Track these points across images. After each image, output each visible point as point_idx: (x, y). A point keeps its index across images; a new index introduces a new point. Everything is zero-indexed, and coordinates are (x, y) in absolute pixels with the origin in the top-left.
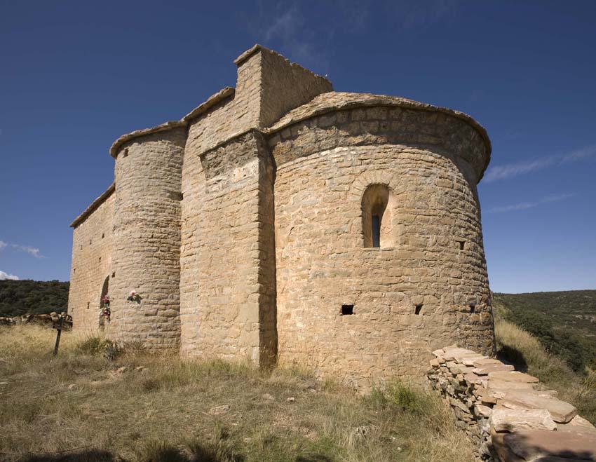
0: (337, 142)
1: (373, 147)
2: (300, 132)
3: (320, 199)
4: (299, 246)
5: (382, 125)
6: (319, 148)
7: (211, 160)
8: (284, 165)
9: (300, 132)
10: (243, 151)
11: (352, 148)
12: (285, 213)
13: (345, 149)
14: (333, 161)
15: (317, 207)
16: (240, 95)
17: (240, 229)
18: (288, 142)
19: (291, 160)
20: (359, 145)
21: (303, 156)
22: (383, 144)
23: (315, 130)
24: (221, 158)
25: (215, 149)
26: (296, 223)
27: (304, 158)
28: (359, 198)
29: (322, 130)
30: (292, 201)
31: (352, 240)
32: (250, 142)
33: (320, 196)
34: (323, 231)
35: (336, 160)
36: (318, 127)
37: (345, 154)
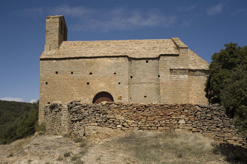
4: (195, 95)
12: (191, 87)
13: (204, 77)
16: (181, 56)
17: (183, 90)
18: (193, 72)
19: (192, 76)
25: (177, 69)
30: (193, 85)
32: (187, 71)
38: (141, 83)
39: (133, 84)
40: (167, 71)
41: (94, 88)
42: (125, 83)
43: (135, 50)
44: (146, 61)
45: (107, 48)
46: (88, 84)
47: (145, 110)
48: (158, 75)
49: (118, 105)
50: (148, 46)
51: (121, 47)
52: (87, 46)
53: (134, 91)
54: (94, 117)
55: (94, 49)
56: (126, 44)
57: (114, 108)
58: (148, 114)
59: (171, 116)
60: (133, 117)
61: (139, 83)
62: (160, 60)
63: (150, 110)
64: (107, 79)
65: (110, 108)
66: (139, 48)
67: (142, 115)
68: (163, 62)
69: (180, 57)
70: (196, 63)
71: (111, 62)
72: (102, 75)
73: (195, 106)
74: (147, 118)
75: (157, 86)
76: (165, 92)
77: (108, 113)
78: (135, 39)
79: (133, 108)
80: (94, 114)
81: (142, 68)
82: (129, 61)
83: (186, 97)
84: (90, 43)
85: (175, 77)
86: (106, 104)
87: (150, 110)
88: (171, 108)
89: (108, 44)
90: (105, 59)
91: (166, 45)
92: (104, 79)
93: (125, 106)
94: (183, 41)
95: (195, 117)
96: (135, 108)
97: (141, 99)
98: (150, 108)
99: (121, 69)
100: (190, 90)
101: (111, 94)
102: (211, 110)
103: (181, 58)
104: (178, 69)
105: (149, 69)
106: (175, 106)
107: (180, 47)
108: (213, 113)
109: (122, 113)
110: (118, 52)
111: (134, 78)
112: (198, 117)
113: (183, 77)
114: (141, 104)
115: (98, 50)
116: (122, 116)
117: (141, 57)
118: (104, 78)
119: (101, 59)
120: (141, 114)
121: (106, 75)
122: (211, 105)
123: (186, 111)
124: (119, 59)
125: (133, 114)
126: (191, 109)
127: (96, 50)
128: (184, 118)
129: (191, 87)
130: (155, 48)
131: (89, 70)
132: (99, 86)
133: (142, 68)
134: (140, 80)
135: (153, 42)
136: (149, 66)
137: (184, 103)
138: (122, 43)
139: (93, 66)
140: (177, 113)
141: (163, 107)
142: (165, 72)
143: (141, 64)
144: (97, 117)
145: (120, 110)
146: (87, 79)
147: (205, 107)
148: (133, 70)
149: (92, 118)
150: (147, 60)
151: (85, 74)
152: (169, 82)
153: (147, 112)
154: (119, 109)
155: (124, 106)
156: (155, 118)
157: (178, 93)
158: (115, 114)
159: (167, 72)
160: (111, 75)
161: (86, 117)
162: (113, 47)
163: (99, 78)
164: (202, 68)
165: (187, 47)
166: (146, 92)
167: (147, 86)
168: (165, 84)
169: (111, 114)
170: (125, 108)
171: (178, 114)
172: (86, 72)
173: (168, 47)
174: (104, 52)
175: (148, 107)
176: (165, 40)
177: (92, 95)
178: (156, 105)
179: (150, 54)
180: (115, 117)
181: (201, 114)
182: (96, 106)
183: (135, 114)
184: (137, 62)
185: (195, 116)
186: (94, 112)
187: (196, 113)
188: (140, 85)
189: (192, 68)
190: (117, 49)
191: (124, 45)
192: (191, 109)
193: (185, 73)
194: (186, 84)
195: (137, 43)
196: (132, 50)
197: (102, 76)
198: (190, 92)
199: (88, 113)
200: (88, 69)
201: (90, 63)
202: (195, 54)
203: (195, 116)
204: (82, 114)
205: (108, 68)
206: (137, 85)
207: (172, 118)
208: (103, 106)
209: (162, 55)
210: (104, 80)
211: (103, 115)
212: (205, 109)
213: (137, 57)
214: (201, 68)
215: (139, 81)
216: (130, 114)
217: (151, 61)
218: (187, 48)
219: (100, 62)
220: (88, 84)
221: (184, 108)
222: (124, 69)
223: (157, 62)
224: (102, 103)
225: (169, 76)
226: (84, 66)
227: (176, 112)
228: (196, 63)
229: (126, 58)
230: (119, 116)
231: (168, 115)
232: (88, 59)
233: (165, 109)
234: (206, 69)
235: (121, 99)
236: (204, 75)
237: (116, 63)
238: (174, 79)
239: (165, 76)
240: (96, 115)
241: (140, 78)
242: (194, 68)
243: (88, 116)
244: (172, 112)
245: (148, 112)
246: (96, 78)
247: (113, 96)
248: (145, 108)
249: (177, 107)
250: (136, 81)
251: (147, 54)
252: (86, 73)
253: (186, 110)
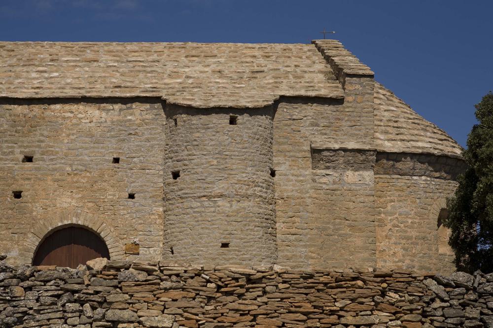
0: (425, 173)
1: (443, 181)
2: (403, 159)
4: (395, 244)
5: (452, 168)
6: (413, 173)
8: (381, 176)
9: (403, 159)
10: (361, 161)
11: (433, 179)
12: (383, 215)
13: (429, 179)
14: (421, 186)
15: (410, 218)
17: (356, 223)
18: (391, 162)
19: (388, 174)
21: (400, 175)
22: (448, 180)
23: (415, 162)
24: (337, 158)
26: (395, 226)
27: (399, 177)
29: (419, 164)
30: (389, 208)
31: (433, 246)
33: (413, 210)
34: (414, 236)
35: (422, 186)
36: (418, 161)
37: (429, 182)
38: (209, 197)
39: (181, 201)
40: (300, 155)
41: (37, 210)
42: (153, 197)
43: (188, 77)
44: (228, 117)
45: (87, 69)
46: (18, 195)
47: (246, 292)
48: (271, 169)
49: (149, 272)
50: (234, 66)
51: (137, 68)
52: (15, 60)
53: (184, 225)
54: (59, 315)
55: (42, 72)
56: (155, 57)
57: (136, 285)
58: (259, 306)
59: (341, 313)
60: (202, 316)
61: (204, 196)
62: (276, 115)
63: (265, 293)
64: (86, 179)
65: (120, 283)
66: (201, 72)
67: (237, 311)
68: (286, 125)
69: (348, 107)
70: (402, 130)
71: (103, 120)
72: (71, 165)
73: (424, 281)
74: (254, 320)
75: (265, 209)
76: (293, 230)
77: (111, 303)
78: (185, 38)
79: (203, 286)
80: (59, 304)
81: (213, 143)
82: (167, 118)
83: (367, 249)
84: (27, 49)
85: (328, 178)
86: (105, 267)
87: (265, 293)
88: (341, 287)
89: (89, 55)
90: (81, 107)
91: (296, 66)
92: (75, 180)
93: (174, 278)
94: (354, 53)
95: (423, 320)
96: (213, 285)
97: (211, 254)
98: (264, 285)
99: (138, 146)
100: (378, 226)
101: (102, 235)
102: (481, 295)
103: (351, 109)
104: (341, 149)
105: (240, 146)
106: (354, 279)
107: (345, 71)
108: (485, 306)
109: (163, 303)
110: (129, 84)
111: (187, 178)
112: (435, 318)
113: (357, 180)
114: (233, 269)
115: (56, 74)
116: (163, 312)
117: (212, 105)
118: (75, 174)
119: (67, 107)
120: (231, 306)
121: (84, 165)
122: (478, 277)
123: (393, 296)
124: (131, 108)
125: (203, 305)
126: (410, 289)
127: (46, 75)
128: (386, 323)
129: (383, 215)
130: (258, 75)
131: (20, 147)
132: (58, 205)
133: (213, 143)
134: (206, 185)
135: (252, 52)
136: (241, 136)
137: (385, 270)
138: (141, 54)
139: (37, 133)
140: (362, 303)
141: (310, 281)
142: (293, 158)
143: (212, 128)
144: (70, 315)
145: (155, 293)
146: (13, 178)
147: (458, 286)
148: (183, 148)
149: (51, 321)
150: (233, 113)
151: (7, 160)
152: (308, 195)
153: (255, 299)
154: (154, 287)
155: (170, 276)
156: (284, 323)
157: (339, 235)
158: (137, 306)
159: (300, 160)
160: (99, 167)
161: (29, 314)
162: (108, 67)
163: (57, 176)
164: (423, 148)
165: (373, 73)
166: (229, 228)
167: (231, 206)
168: (292, 201)
169: (124, 306)
170: (174, 285)
171: (363, 307)
172: (12, 152)
173: (305, 72)
174: (76, 84)
175: (259, 281)
176: (291, 46)
177: (30, 235)
178: (285, 276)
179: (242, 94)
180: (140, 317)
181: (443, 308)
182: (67, 277)
183: (212, 307)
184: (196, 120)
185: (424, 314)
186: (58, 296)
187: (428, 304)
188: (206, 204)
189: (389, 146)
190: (122, 75)
191: (147, 61)
192: (410, 289)
193: (362, 166)
194: (365, 204)
195: (194, 52)
196: (175, 78)
197: (68, 169)
198: (381, 233)
199: (38, 300)
200: (20, 144)
201: (26, 122)
202: (396, 101)
203: (424, 314)
204: (14, 303)
205: (90, 139)
206: (195, 204)
207: (343, 320)
208: (94, 276)
209: (283, 99)
210: (76, 182)
211: (94, 308)
212: (458, 290)
213: (197, 103)
214: (419, 148)
215: (205, 188)
216: (193, 308)
217: (246, 118)
218: (371, 76)
219: (64, 118)
220: (18, 195)
221: (385, 285)
222: (148, 144)
223: (268, 121)
224: (90, 263)
225: (307, 173)
226: (6, 131)
227: (356, 299)
228: (402, 130)
229: (158, 105)
230: (155, 312)
231: (331, 311)
232: (20, 104)
233: (318, 290)
234: (436, 152)
235: (138, 254)
236: (428, 173)
237: (120, 123)
238: (324, 186)
239: (293, 175)
240: (67, 309)
241: (209, 179)
242: (393, 147)
243: (38, 312)
244: (343, 299)
245: (259, 299)
246: (47, 175)
247: (109, 242)
248: (247, 286)
249: (360, 283)
250: (191, 189)
251: (232, 94)
252: (11, 156)
253: (392, 294)
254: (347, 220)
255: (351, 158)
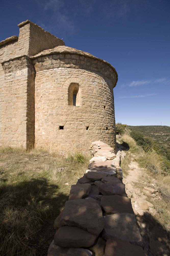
0: (60, 65)
1: (74, 69)
2: (45, 60)
3: (53, 86)
4: (44, 103)
6: (53, 67)
7: (6, 66)
9: (45, 60)
12: (39, 91)
13: (63, 68)
14: (58, 73)
15: (51, 89)
16: (20, 40)
17: (19, 95)
18: (41, 63)
20: (68, 68)
21: (47, 69)
22: (78, 68)
25: (8, 61)
27: (47, 70)
28: (67, 87)
29: (54, 60)
30: (42, 86)
31: (64, 102)
33: (53, 85)
35: (59, 72)
36: (52, 59)
37: (63, 70)
113: (21, 74)
193: (22, 66)
254: (16, 94)
255: (16, 64)
